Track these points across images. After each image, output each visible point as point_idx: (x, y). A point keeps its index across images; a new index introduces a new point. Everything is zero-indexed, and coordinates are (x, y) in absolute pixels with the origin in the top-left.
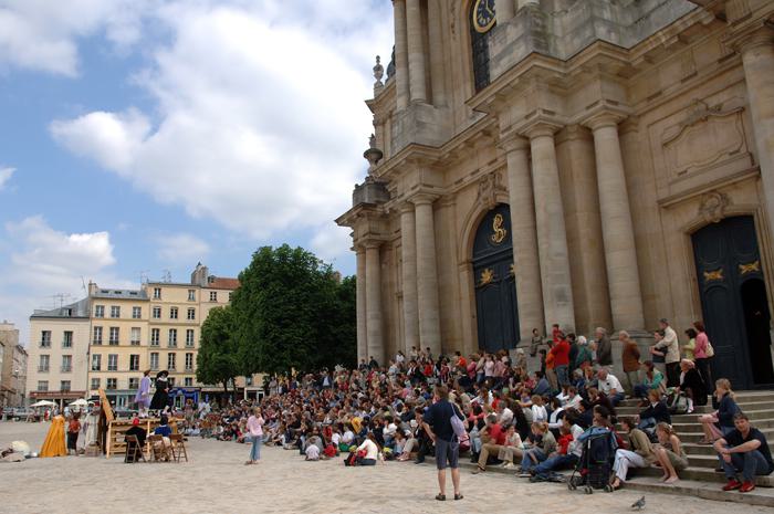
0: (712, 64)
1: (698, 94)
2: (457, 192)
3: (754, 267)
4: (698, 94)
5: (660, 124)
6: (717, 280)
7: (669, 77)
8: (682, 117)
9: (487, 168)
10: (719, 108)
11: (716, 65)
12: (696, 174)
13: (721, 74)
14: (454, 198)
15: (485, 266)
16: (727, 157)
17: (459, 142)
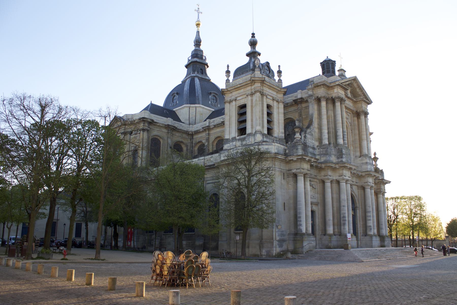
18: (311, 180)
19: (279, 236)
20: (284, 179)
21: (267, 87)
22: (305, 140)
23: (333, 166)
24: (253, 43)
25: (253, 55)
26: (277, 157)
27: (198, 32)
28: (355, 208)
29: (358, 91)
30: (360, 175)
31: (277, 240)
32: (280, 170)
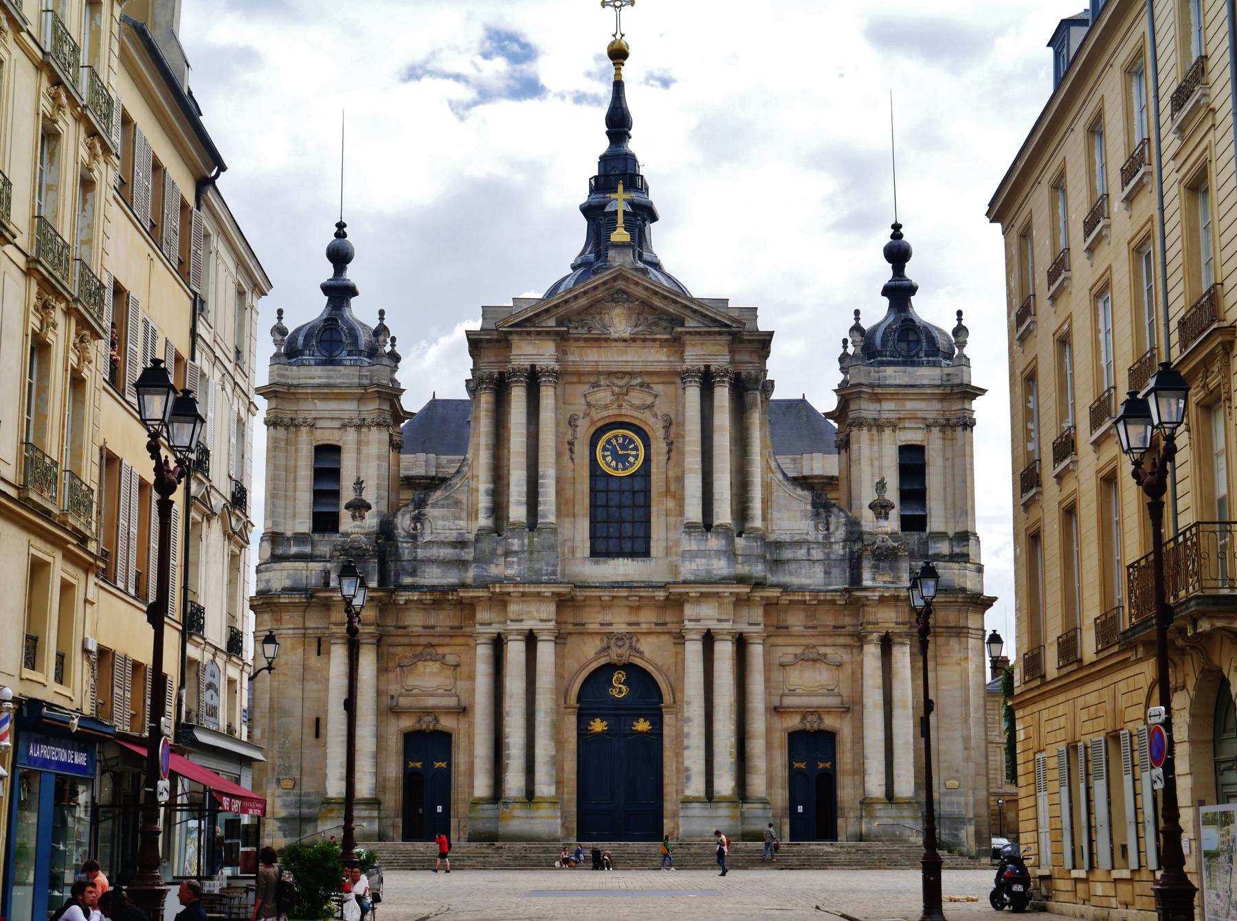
0: (827, 626)
1: (813, 641)
2: (570, 634)
3: (828, 765)
4: (813, 641)
5: (779, 648)
6: (799, 769)
7: (796, 620)
8: (799, 651)
9: (624, 626)
10: (825, 655)
11: (830, 629)
12: (800, 695)
13: (831, 636)
14: (565, 638)
15: (597, 716)
16: (825, 691)
17: (607, 594)
18: (433, 643)
19: (285, 806)
20: (319, 654)
21: (313, 399)
22: (415, 529)
23: (480, 594)
24: (339, 256)
25: (339, 293)
26: (276, 601)
27: (618, 86)
28: (661, 709)
29: (661, 305)
30: (662, 598)
31: (278, 816)
32: (303, 631)
